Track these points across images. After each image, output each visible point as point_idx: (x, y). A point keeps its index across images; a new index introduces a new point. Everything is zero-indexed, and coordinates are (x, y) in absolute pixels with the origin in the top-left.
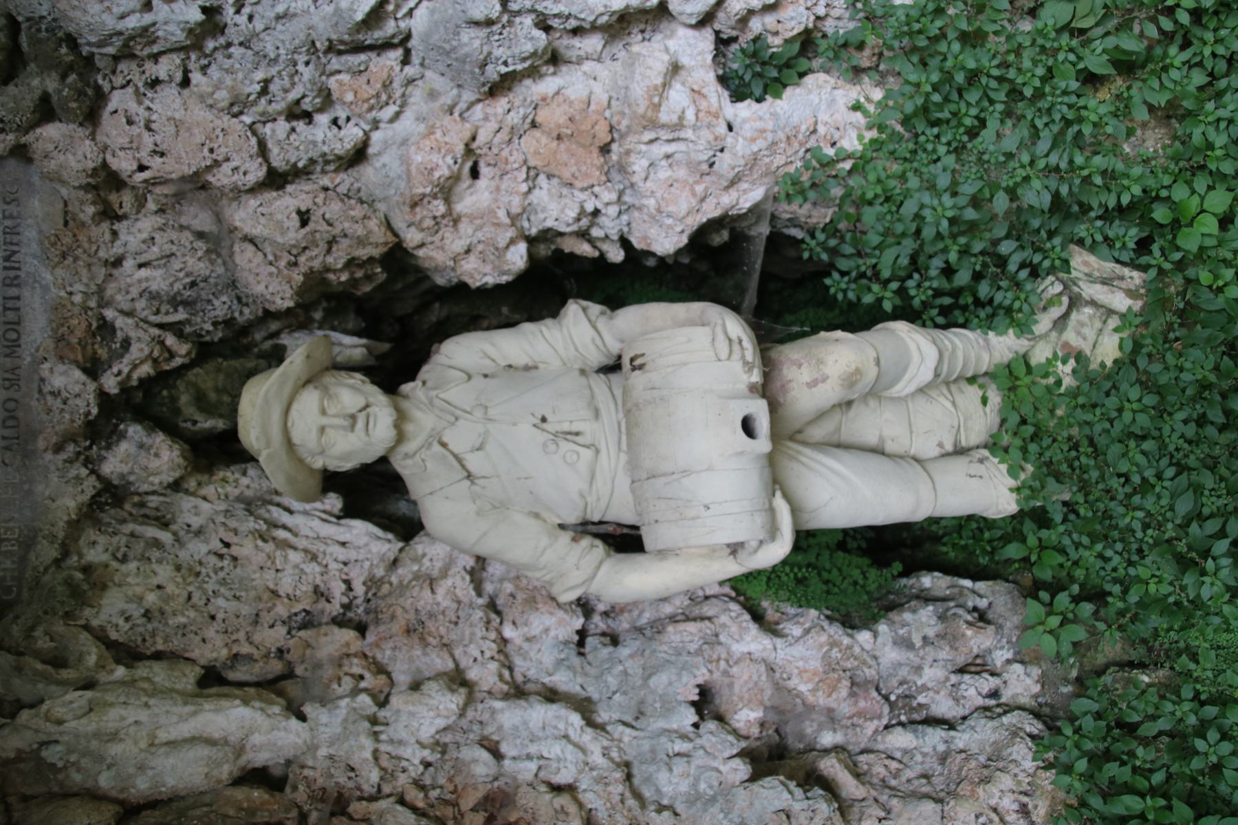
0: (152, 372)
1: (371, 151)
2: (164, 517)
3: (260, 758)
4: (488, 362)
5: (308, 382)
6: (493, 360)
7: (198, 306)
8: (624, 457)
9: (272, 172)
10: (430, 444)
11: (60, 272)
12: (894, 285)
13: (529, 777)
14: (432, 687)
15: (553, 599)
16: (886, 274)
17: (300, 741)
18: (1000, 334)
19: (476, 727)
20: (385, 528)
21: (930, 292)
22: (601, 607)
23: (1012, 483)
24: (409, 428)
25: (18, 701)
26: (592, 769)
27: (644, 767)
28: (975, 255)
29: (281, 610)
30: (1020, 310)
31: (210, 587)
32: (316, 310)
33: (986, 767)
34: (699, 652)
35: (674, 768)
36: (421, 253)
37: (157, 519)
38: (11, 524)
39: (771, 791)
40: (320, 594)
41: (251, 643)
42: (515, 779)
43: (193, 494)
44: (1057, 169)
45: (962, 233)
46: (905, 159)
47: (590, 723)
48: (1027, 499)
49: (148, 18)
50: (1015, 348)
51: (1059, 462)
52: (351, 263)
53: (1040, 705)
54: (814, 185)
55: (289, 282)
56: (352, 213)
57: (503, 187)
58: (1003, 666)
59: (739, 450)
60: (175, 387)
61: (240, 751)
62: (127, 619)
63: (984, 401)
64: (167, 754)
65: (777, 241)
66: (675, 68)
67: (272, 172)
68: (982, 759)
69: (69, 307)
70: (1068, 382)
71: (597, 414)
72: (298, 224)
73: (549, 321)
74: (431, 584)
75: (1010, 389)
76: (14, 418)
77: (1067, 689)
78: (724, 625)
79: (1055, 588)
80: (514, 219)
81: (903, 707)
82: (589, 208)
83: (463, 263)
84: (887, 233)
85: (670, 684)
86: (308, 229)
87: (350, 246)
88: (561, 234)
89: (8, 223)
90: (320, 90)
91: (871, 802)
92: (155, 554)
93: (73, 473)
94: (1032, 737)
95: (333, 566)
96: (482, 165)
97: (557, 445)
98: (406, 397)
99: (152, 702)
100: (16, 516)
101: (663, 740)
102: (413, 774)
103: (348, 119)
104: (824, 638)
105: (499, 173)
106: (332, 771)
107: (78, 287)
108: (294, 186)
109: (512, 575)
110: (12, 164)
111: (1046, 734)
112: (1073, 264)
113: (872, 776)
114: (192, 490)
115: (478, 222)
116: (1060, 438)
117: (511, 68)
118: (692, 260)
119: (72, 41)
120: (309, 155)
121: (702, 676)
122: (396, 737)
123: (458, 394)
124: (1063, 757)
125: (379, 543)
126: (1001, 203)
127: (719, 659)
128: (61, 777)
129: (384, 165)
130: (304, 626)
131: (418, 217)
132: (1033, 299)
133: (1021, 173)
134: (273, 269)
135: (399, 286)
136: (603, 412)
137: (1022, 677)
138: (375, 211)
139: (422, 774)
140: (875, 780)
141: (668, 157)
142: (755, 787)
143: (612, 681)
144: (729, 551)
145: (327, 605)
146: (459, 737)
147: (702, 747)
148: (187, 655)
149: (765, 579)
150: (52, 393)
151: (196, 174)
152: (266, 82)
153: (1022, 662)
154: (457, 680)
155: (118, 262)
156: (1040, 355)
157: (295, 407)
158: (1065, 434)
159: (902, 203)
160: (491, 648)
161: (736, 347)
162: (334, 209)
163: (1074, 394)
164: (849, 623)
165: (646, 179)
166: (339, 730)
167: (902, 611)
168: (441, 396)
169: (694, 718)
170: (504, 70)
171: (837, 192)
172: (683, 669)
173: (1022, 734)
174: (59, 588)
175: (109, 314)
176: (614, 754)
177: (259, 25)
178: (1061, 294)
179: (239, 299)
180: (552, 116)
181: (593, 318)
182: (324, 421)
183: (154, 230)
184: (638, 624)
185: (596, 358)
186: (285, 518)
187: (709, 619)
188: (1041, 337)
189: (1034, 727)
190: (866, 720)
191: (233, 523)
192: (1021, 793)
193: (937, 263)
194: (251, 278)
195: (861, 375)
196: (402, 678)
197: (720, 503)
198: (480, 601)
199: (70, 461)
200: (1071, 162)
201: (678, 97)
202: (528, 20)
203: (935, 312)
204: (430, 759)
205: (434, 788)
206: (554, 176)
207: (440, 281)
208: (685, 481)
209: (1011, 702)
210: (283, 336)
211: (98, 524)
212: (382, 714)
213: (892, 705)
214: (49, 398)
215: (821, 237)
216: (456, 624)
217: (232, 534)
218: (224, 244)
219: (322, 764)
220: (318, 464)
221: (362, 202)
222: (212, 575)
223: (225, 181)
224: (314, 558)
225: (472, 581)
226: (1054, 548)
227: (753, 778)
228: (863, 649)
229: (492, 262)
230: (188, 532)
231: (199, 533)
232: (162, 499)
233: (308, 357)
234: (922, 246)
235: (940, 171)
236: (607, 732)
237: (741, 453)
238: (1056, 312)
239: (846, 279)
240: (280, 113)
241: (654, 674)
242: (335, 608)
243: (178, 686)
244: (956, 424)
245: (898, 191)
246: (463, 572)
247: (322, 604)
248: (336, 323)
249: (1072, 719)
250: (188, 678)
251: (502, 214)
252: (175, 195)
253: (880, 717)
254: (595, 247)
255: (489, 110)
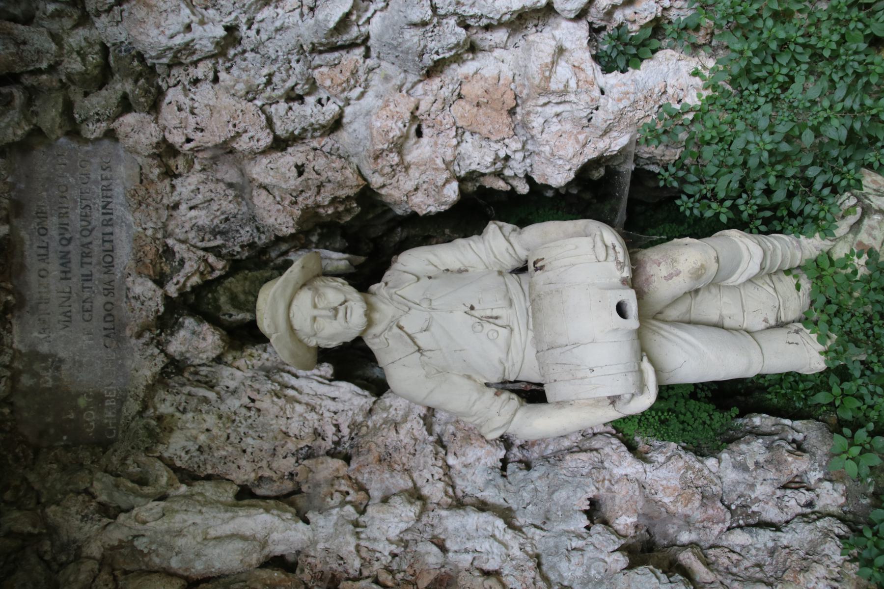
0: (200, 281)
1: (345, 120)
2: (211, 381)
3: (278, 550)
4: (432, 268)
5: (304, 285)
6: (436, 266)
7: (230, 235)
8: (531, 334)
9: (276, 139)
10: (391, 328)
11: (137, 214)
12: (728, 203)
13: (467, 565)
14: (396, 501)
15: (482, 437)
16: (721, 195)
17: (305, 538)
18: (809, 237)
19: (428, 529)
20: (363, 387)
21: (755, 207)
22: (518, 442)
23: (821, 348)
24: (376, 316)
25: (119, 507)
26: (511, 560)
27: (550, 558)
28: (789, 179)
29: (291, 446)
30: (824, 219)
31: (242, 430)
32: (313, 235)
33: (804, 559)
34: (589, 475)
35: (572, 559)
36: (383, 192)
37: (206, 383)
38: (111, 387)
39: (644, 577)
40: (318, 434)
41: (271, 469)
42: (456, 566)
43: (230, 366)
44: (851, 110)
45: (779, 162)
46: (734, 110)
47: (511, 526)
48: (833, 359)
49: (189, 37)
50: (821, 247)
51: (857, 332)
52: (334, 201)
53: (845, 512)
54: (665, 132)
55: (291, 215)
56: (334, 165)
57: (439, 142)
58: (816, 483)
59: (615, 327)
60: (216, 291)
61: (264, 544)
62: (187, 452)
63: (798, 287)
64: (215, 546)
65: (640, 175)
66: (561, 51)
67: (276, 139)
68: (802, 553)
69: (144, 238)
70: (862, 271)
71: (511, 303)
72: (296, 174)
73: (475, 237)
74: (396, 427)
75: (817, 278)
76: (110, 315)
77: (866, 501)
78: (607, 455)
79: (855, 425)
80: (448, 165)
81: (741, 515)
82: (502, 154)
83: (413, 197)
84: (721, 164)
85: (568, 498)
86: (303, 177)
87: (333, 189)
88: (483, 175)
89: (105, 183)
90: (308, 79)
91: (718, 584)
92: (205, 407)
93: (149, 352)
94: (839, 536)
95: (327, 415)
96: (424, 127)
97: (482, 326)
98: (374, 294)
99: (204, 510)
100: (114, 382)
101: (564, 538)
102: (384, 562)
103: (328, 99)
104: (681, 464)
105: (436, 132)
106: (328, 559)
107: (150, 225)
108: (292, 148)
109: (453, 420)
110: (106, 143)
111: (851, 535)
112: (863, 182)
113: (718, 565)
114: (229, 362)
115: (423, 168)
116: (857, 314)
117: (441, 56)
118: (579, 192)
119: (140, 57)
120: (302, 125)
121: (592, 492)
122: (372, 536)
123: (411, 291)
124: (865, 554)
125: (359, 398)
126: (808, 138)
127: (604, 480)
128: (146, 559)
129: (355, 130)
130: (308, 457)
131: (380, 166)
132: (834, 210)
133: (823, 114)
134: (280, 207)
135: (371, 216)
136: (515, 301)
137: (831, 492)
138: (350, 163)
139: (391, 562)
140: (721, 568)
141: (558, 115)
142: (631, 573)
143: (526, 496)
144: (609, 401)
145: (323, 442)
146: (416, 536)
147: (592, 544)
148: (228, 477)
149: (637, 420)
150: (134, 298)
151: (225, 142)
152: (270, 76)
153: (830, 481)
154: (415, 495)
155: (176, 206)
156: (840, 251)
157: (295, 303)
158: (861, 310)
159: (732, 142)
160: (439, 472)
161: (611, 252)
162: (320, 163)
163: (868, 280)
164: (700, 452)
165: (542, 132)
166: (332, 530)
167: (739, 443)
168: (398, 292)
169: (587, 523)
170: (436, 57)
171: (683, 136)
172: (577, 487)
173: (832, 535)
174: (141, 431)
175: (170, 242)
176: (529, 549)
177: (264, 36)
178: (855, 205)
179: (258, 229)
180: (472, 90)
181: (507, 234)
182: (316, 312)
183: (199, 183)
184: (545, 454)
185: (510, 263)
186: (293, 381)
187: (596, 450)
188: (840, 238)
189: (840, 529)
190: (713, 523)
191: (257, 386)
192: (832, 579)
193: (760, 185)
194: (265, 214)
195: (705, 270)
196: (376, 494)
197: (602, 367)
198: (431, 439)
199: (147, 344)
200: (862, 105)
201: (563, 71)
202: (452, 21)
203: (759, 222)
204: (396, 551)
205: (399, 572)
206: (475, 133)
207: (399, 212)
208: (575, 351)
209: (823, 510)
210: (290, 254)
211: (166, 386)
212: (362, 519)
213: (733, 513)
214: (133, 301)
215: (672, 170)
216: (414, 455)
217: (255, 393)
218: (247, 190)
219: (320, 555)
220: (313, 343)
221: (340, 157)
222: (243, 422)
223: (245, 147)
224: (313, 409)
225: (425, 424)
226: (853, 396)
227: (630, 567)
228: (710, 471)
229: (434, 196)
230: (227, 392)
231: (234, 392)
232: (209, 369)
233: (303, 267)
234: (748, 174)
235: (760, 116)
236: (523, 533)
237: (617, 329)
238: (852, 219)
239: (692, 200)
240: (280, 97)
241: (557, 490)
242: (328, 445)
243: (222, 499)
244: (777, 304)
245: (729, 133)
246: (418, 418)
247: (320, 441)
248: (328, 244)
249: (871, 525)
250: (228, 493)
251: (439, 162)
252: (211, 158)
253: (724, 521)
254: (507, 183)
255: (427, 87)
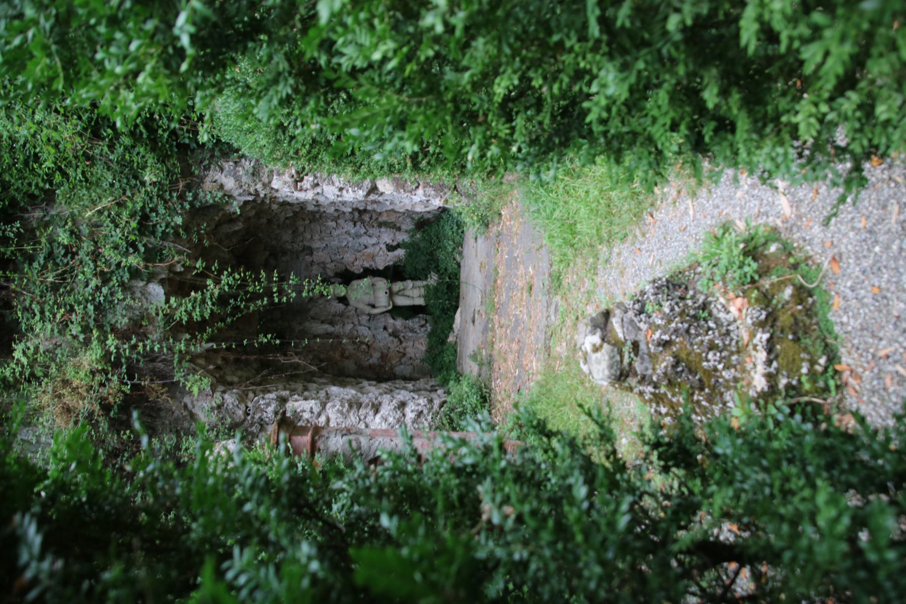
164: (406, 319)
